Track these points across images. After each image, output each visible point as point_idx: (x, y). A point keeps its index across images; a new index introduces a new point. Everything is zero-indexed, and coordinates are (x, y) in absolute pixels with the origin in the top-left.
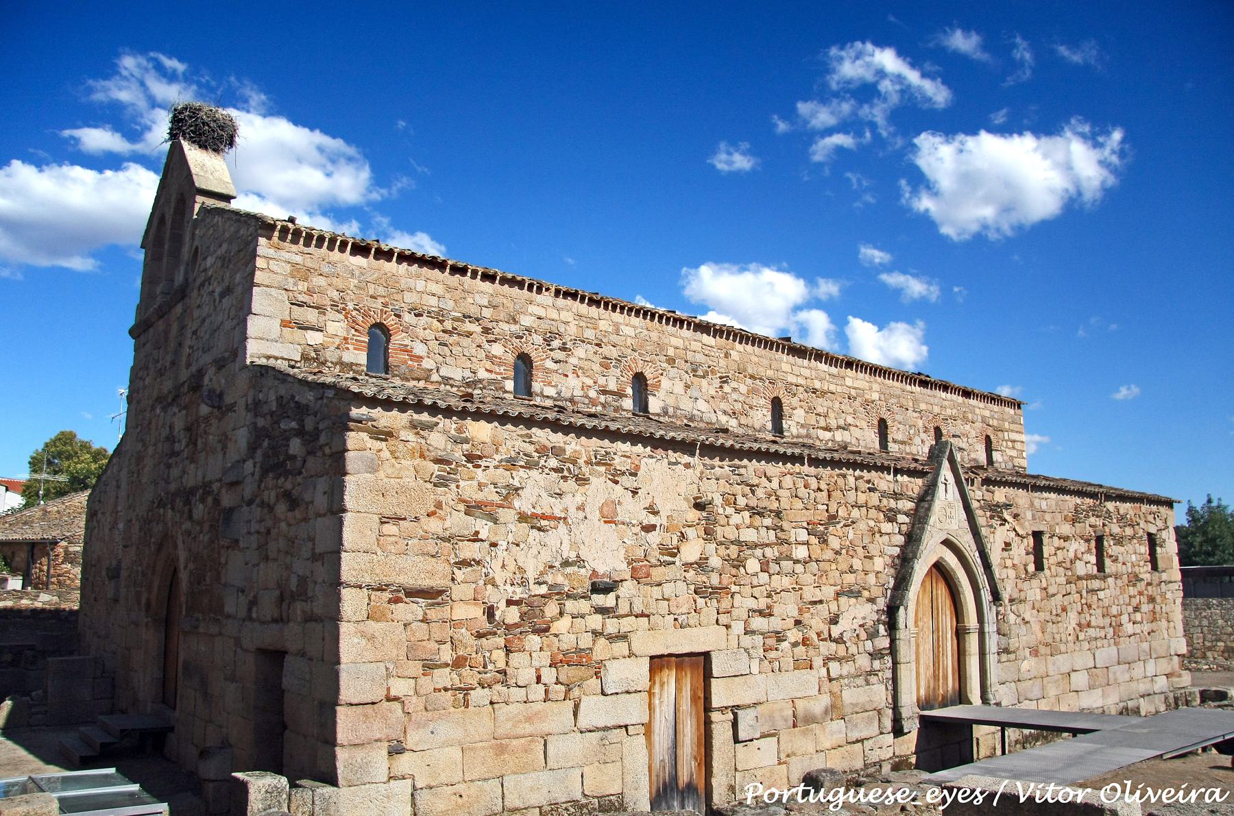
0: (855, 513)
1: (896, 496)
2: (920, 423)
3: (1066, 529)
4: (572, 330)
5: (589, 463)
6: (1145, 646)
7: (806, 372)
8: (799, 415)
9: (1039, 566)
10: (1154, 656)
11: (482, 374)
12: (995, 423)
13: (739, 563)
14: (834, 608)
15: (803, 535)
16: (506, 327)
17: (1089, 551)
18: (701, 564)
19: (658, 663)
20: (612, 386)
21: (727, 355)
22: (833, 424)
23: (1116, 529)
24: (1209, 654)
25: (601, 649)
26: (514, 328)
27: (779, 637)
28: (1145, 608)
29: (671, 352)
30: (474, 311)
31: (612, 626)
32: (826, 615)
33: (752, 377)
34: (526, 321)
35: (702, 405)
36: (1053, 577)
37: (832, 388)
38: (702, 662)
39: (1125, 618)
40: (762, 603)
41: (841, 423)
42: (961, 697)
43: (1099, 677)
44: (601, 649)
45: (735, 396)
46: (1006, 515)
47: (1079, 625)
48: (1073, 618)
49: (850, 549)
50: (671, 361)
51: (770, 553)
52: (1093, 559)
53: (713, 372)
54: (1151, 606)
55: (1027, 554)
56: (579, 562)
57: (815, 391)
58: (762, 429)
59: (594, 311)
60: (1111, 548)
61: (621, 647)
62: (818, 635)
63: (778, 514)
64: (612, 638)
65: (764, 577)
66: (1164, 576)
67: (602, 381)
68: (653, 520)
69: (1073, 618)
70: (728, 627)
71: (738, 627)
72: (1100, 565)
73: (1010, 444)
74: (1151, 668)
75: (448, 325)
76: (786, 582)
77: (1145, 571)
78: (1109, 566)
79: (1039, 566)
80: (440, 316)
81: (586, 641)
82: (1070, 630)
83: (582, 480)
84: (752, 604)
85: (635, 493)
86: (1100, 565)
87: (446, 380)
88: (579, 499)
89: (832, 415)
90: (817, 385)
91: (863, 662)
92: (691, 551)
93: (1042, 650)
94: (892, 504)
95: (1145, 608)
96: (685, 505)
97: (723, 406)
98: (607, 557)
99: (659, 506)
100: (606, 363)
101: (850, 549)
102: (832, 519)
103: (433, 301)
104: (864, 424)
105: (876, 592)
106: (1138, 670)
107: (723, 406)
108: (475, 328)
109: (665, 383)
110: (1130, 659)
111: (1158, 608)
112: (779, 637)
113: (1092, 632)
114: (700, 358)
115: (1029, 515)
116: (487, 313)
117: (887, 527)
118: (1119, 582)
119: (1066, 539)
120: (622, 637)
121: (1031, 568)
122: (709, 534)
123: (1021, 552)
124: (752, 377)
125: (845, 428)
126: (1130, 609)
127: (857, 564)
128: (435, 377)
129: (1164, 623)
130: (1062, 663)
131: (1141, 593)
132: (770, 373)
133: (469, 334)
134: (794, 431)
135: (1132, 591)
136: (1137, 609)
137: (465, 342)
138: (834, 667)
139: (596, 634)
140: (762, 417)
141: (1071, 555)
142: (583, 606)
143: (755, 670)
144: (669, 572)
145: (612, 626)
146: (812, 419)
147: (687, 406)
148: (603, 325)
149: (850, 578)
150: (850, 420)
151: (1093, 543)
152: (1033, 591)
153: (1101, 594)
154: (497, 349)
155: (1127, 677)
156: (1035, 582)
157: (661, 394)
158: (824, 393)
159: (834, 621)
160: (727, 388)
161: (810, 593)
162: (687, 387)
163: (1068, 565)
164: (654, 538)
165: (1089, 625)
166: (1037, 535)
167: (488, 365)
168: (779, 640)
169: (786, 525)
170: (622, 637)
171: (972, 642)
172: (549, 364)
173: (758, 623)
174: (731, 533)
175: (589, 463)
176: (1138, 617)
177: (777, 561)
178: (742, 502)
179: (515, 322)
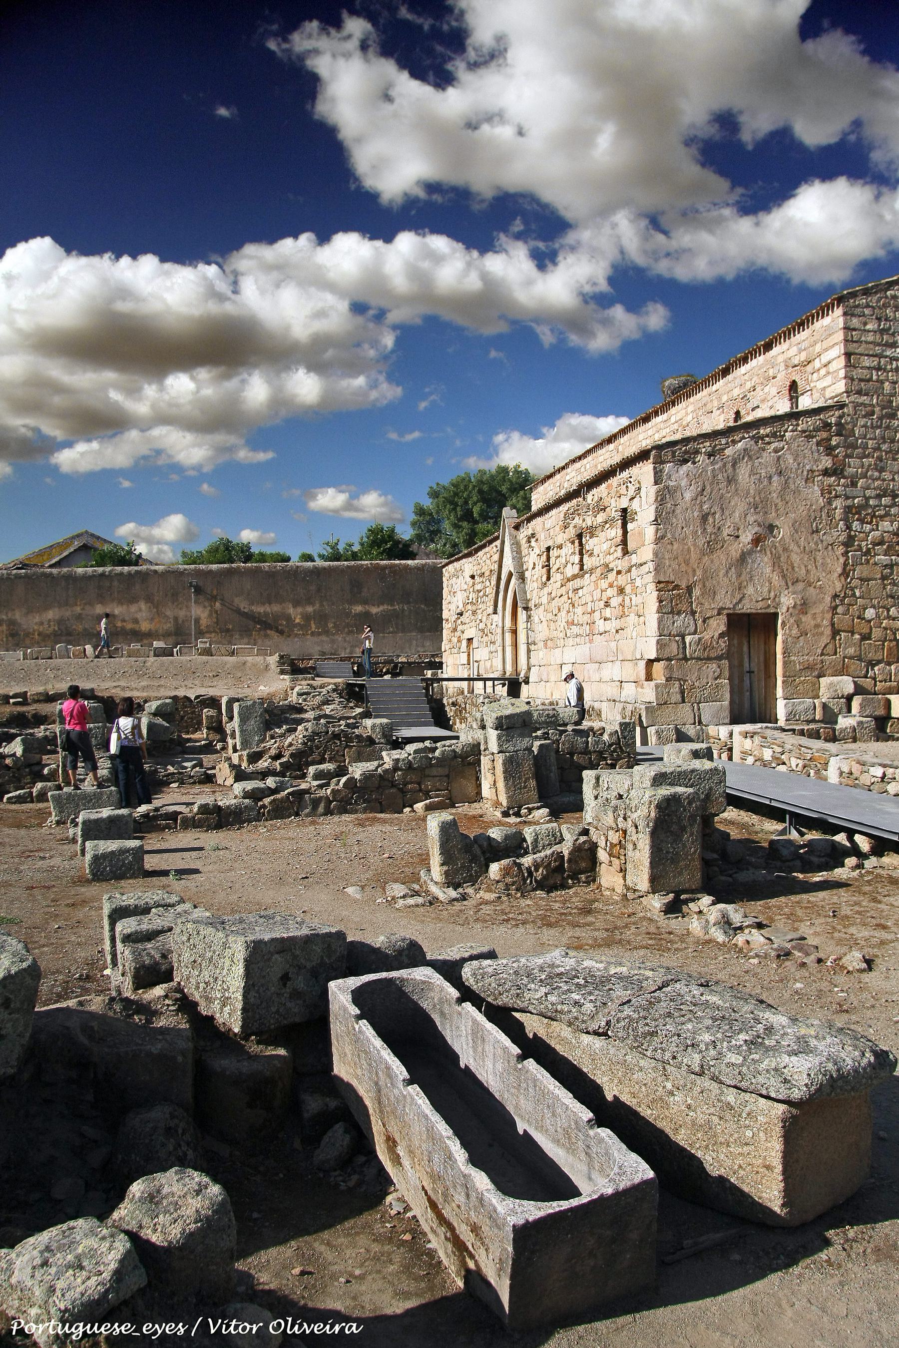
12: (803, 356)
28: (615, 602)
47: (567, 622)
54: (620, 598)
66: (634, 559)
110: (599, 659)
111: (627, 599)
115: (543, 537)
126: (602, 604)
131: (611, 586)
156: (546, 590)
166: (548, 549)
176: (608, 612)
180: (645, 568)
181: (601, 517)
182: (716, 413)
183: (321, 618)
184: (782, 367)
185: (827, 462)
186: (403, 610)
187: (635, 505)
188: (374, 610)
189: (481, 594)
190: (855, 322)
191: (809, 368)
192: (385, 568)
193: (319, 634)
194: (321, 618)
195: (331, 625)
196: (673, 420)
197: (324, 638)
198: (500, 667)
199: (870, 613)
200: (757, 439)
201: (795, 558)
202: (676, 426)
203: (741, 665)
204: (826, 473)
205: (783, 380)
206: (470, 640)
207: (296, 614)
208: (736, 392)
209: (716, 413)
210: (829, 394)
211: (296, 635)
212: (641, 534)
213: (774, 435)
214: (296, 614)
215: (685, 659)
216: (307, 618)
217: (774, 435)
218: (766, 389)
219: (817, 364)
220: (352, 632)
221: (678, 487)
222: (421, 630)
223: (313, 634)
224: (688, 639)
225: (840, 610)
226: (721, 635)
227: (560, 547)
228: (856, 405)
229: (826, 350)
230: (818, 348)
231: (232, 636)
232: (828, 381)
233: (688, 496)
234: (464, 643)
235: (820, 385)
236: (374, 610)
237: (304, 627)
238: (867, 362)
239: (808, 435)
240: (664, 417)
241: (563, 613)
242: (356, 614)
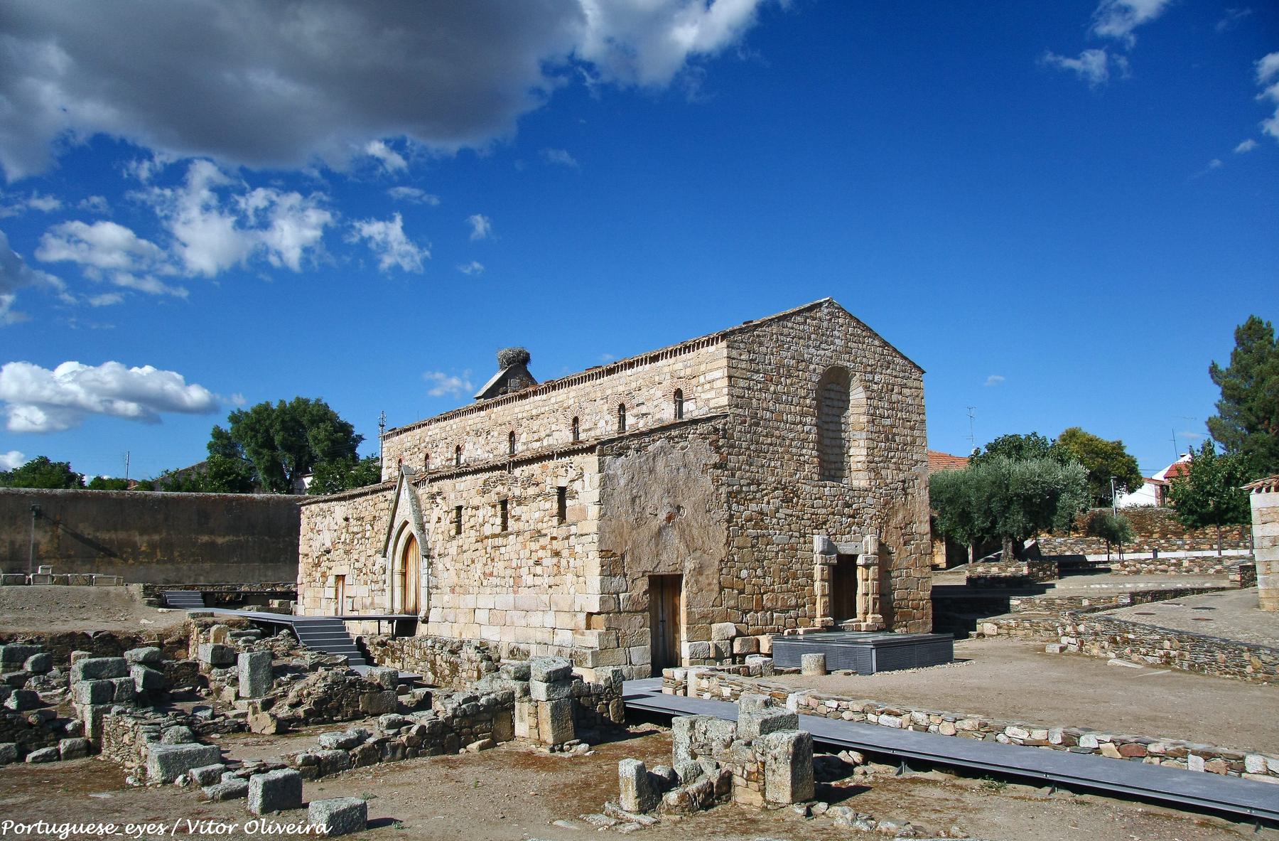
2: (605, 407)
3: (476, 501)
6: (545, 598)
8: (524, 438)
9: (459, 532)
10: (554, 608)
12: (689, 371)
22: (543, 434)
23: (517, 491)
35: (479, 452)
36: (468, 537)
39: (524, 571)
41: (548, 432)
48: (478, 569)
52: (499, 521)
54: (555, 560)
60: (514, 510)
69: (478, 569)
72: (505, 527)
73: (707, 386)
74: (549, 620)
79: (459, 532)
86: (505, 527)
90: (534, 412)
93: (457, 589)
95: (549, 561)
98: (328, 545)
104: (562, 427)
106: (536, 619)
111: (563, 562)
113: (493, 580)
115: (452, 496)
118: (520, 538)
119: (477, 508)
121: (453, 532)
123: (447, 525)
126: (531, 562)
129: (570, 577)
130: (469, 601)
131: (543, 548)
135: (534, 546)
136: (537, 563)
140: (504, 447)
141: (481, 520)
151: (499, 508)
152: (453, 548)
153: (503, 550)
155: (523, 622)
156: (455, 543)
165: (491, 574)
166: (459, 508)
176: (539, 570)
180: (589, 539)
181: (532, 491)
182: (599, 402)
183: (167, 547)
184: (668, 376)
185: (716, 458)
186: (248, 541)
187: (577, 486)
188: (220, 540)
189: (359, 536)
190: (734, 353)
191: (694, 382)
192: (232, 500)
193: (165, 562)
194: (167, 547)
195: (176, 554)
196: (553, 400)
197: (169, 566)
198: (388, 605)
199: (744, 573)
200: (670, 438)
201: (695, 532)
202: (556, 406)
203: (656, 616)
204: (715, 466)
205: (669, 385)
206: (341, 578)
207: (142, 542)
208: (621, 389)
209: (599, 402)
210: (712, 404)
211: (141, 563)
212: (583, 511)
213: (681, 437)
214: (142, 542)
215: (620, 612)
216: (153, 546)
217: (681, 437)
218: (652, 391)
219: (702, 379)
220: (195, 561)
221: (615, 475)
222: (264, 561)
223: (158, 562)
224: (622, 596)
225: (724, 571)
226: (645, 593)
227: (477, 508)
228: (736, 415)
229: (711, 371)
230: (703, 368)
231: (73, 562)
232: (712, 394)
233: (622, 482)
234: (331, 580)
235: (704, 396)
236: (220, 540)
237: (150, 555)
238: (742, 383)
239: (704, 437)
240: (544, 397)
241: (479, 566)
242: (203, 544)
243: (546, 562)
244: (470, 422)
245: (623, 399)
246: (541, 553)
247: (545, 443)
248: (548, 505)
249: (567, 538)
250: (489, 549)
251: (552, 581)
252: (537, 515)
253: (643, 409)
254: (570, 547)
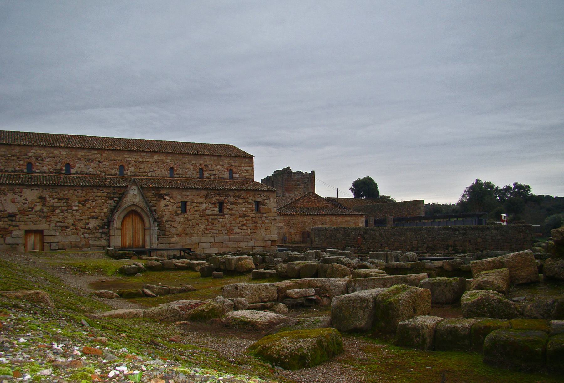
0: (96, 198)
1: (114, 194)
2: (192, 167)
3: (201, 200)
4: (45, 154)
5: (8, 191)
7: (136, 157)
9: (184, 210)
11: (17, 169)
12: (236, 164)
13: (54, 210)
14: (87, 221)
15: (77, 204)
16: (24, 157)
17: (215, 207)
18: (41, 211)
19: (28, 232)
20: (58, 167)
21: (101, 155)
22: (147, 170)
24: (420, 249)
25: (11, 228)
26: (26, 157)
27: (67, 227)
29: (79, 157)
30: (14, 154)
31: (14, 224)
32: (84, 223)
33: (111, 160)
34: (30, 154)
37: (147, 160)
38: (41, 232)
40: (61, 219)
41: (152, 170)
42: (144, 247)
43: (212, 245)
44: (11, 228)
45: (104, 166)
46: (166, 197)
49: (95, 207)
50: (79, 159)
51: (63, 208)
52: (217, 209)
53: (96, 160)
54: (253, 225)
55: (177, 208)
56: (5, 211)
57: (139, 162)
58: (115, 175)
59: (52, 150)
61: (17, 228)
62: (81, 227)
63: (68, 199)
64: (14, 226)
65: (62, 214)
67: (55, 167)
68: (26, 202)
69: (202, 227)
70: (49, 225)
71: (53, 225)
73: (245, 171)
74: (251, 244)
75: (7, 158)
76: (69, 215)
77: (252, 214)
78: (226, 211)
80: (5, 156)
81: (7, 226)
82: (201, 230)
83: (6, 194)
84: (58, 220)
85: (21, 196)
87: (7, 171)
88: (5, 198)
89: (146, 168)
90: (141, 160)
91: (99, 235)
92: (38, 208)
94: (112, 195)
95: (250, 225)
96: (36, 198)
97: (99, 169)
99: (28, 198)
100: (56, 162)
101: (95, 207)
102: (87, 200)
103: (3, 153)
105: (103, 218)
107: (99, 169)
108: (15, 158)
109: (77, 165)
112: (67, 227)
114: (90, 157)
116: (18, 154)
117: (110, 201)
119: (201, 203)
120: (18, 226)
121: (179, 212)
122: (44, 205)
124: (111, 160)
125: (154, 171)
126: (240, 225)
127: (96, 210)
128: (4, 171)
131: (247, 220)
132: (119, 158)
133: (13, 160)
134: (129, 174)
135: (241, 219)
137: (12, 161)
138: (86, 236)
139: (10, 225)
142: (6, 219)
143: (58, 234)
144: (31, 213)
145: (14, 224)
146: (138, 170)
147: (85, 170)
148: (55, 152)
149: (94, 214)
150: (155, 169)
151: (217, 205)
152: (181, 219)
154: (21, 162)
157: (76, 168)
158: (143, 162)
159: (87, 224)
160: (101, 164)
161: (77, 218)
162: (85, 165)
163: (201, 210)
164: (26, 206)
165: (212, 229)
167: (19, 166)
168: (67, 228)
169: (70, 202)
170: (18, 226)
171: (147, 232)
172: (37, 164)
173: (59, 224)
174: (50, 204)
175: (8, 191)
176: (244, 227)
177: (67, 210)
178: (55, 197)
179: (27, 155)
181: (240, 200)
184: (226, 164)
191: (239, 168)
202: (157, 160)
210: (247, 177)
227: (201, 203)
243: (248, 225)
244: (83, 154)
245: (202, 166)
246: (245, 222)
247: (149, 174)
248: (250, 206)
249: (261, 217)
250: (210, 220)
251: (252, 231)
252: (244, 209)
253: (214, 173)
254: (262, 221)
